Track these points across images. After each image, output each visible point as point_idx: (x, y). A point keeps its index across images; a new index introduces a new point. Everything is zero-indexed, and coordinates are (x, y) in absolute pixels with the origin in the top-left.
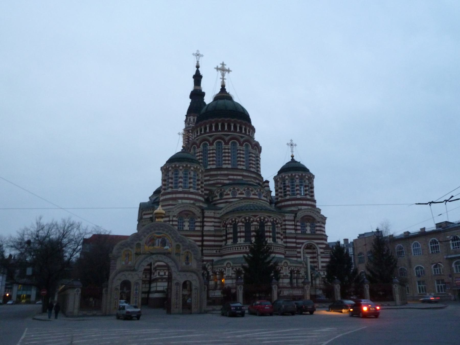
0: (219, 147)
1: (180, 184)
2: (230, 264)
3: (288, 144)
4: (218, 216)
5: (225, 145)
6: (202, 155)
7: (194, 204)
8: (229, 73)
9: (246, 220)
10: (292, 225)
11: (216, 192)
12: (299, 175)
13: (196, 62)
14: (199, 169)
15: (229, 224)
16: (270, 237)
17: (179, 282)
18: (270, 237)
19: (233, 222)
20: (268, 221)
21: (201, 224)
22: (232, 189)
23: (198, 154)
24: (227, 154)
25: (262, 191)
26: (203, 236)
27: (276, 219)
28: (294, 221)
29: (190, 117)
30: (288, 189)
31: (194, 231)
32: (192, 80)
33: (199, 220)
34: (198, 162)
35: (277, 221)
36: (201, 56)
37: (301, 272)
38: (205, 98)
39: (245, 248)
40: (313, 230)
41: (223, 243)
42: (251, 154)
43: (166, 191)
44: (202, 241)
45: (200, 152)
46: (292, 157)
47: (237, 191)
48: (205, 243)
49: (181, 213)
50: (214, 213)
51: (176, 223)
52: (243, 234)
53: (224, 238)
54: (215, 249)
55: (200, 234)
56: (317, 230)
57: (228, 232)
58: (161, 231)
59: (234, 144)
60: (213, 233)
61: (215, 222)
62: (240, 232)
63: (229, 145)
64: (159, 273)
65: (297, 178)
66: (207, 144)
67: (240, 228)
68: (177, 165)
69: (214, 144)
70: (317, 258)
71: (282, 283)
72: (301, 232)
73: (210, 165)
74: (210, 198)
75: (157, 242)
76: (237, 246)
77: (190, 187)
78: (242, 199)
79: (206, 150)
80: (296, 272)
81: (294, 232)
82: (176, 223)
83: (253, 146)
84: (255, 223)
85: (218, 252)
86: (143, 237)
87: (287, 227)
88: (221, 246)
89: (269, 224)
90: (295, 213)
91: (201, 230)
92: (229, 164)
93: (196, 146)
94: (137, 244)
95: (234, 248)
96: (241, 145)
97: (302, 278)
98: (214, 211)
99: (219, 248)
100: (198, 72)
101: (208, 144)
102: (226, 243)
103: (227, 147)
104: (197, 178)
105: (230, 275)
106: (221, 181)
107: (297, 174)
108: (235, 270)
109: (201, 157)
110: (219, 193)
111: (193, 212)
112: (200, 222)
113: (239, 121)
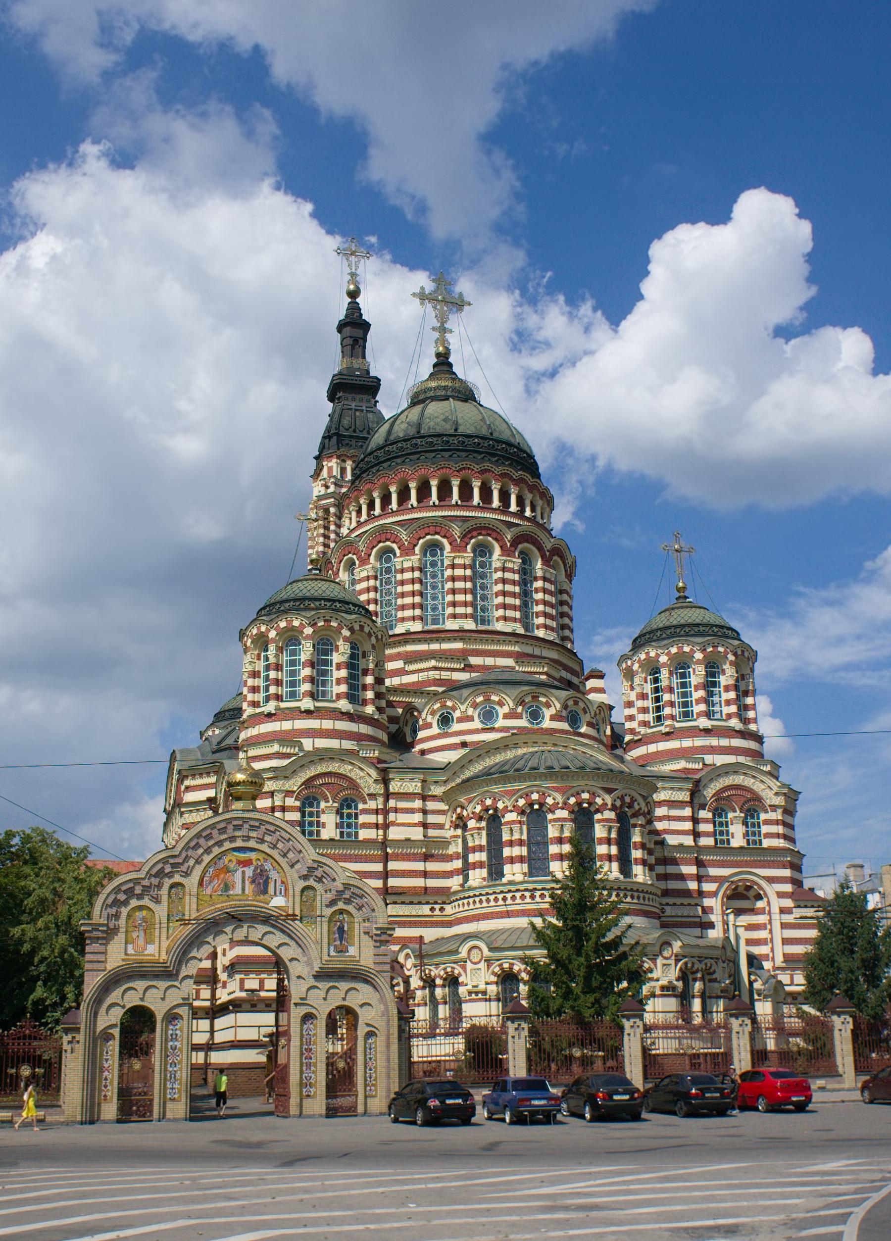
0: (432, 559)
2: (480, 949)
5: (453, 555)
6: (376, 589)
11: (426, 711)
13: (349, 277)
14: (370, 635)
15: (472, 818)
16: (609, 858)
17: (314, 1011)
23: (364, 585)
26: (386, 858)
27: (633, 800)
28: (691, 803)
29: (330, 464)
33: (372, 805)
34: (367, 611)
35: (636, 807)
37: (714, 976)
39: (528, 897)
40: (754, 834)
41: (454, 883)
43: (258, 710)
45: (368, 578)
47: (497, 707)
48: (392, 882)
50: (424, 781)
54: (428, 903)
57: (470, 844)
58: (252, 844)
61: (425, 812)
62: (511, 844)
63: (465, 551)
64: (242, 981)
66: (392, 551)
67: (511, 830)
69: (417, 549)
70: (769, 927)
71: (655, 1012)
72: (716, 840)
73: (403, 620)
74: (408, 730)
75: (238, 876)
76: (502, 892)
78: (513, 734)
79: (388, 571)
80: (699, 975)
81: (693, 844)
83: (548, 554)
85: (437, 912)
86: (191, 862)
88: (444, 892)
89: (612, 815)
91: (380, 837)
92: (466, 616)
93: (354, 557)
94: (172, 886)
95: (492, 897)
97: (719, 994)
98: (422, 777)
101: (398, 552)
102: (466, 879)
103: (457, 561)
105: (482, 987)
106: (443, 673)
108: (497, 970)
109: (372, 595)
110: (437, 717)
112: (377, 812)
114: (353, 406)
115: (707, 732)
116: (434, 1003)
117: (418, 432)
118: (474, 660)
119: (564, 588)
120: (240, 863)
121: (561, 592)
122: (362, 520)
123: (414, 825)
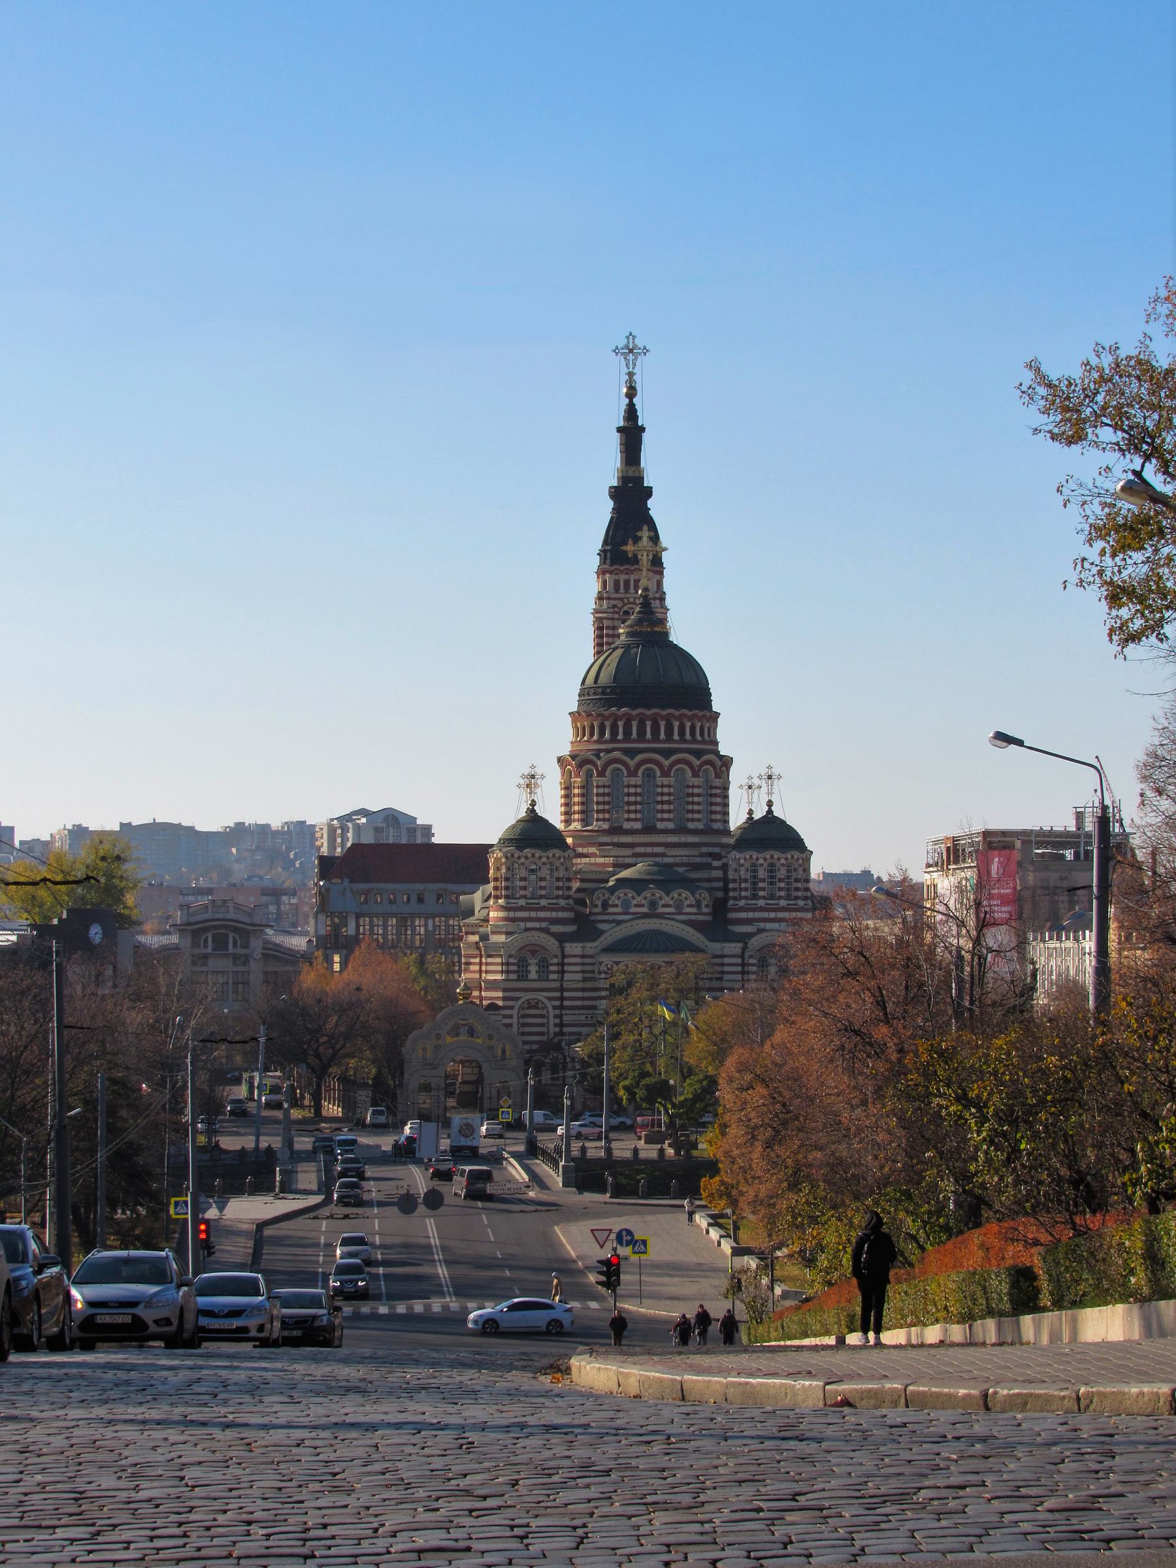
4: (591, 952)
10: (737, 965)
12: (765, 859)
13: (627, 377)
14: (559, 858)
19: (608, 969)
22: (622, 895)
24: (632, 799)
29: (607, 576)
30: (743, 885)
31: (548, 980)
32: (614, 442)
33: (555, 961)
36: (640, 354)
42: (690, 791)
44: (562, 999)
46: (770, 804)
48: (566, 1003)
49: (522, 948)
51: (514, 968)
55: (556, 985)
59: (649, 774)
60: (580, 985)
61: (583, 964)
63: (636, 776)
65: (761, 865)
77: (541, 897)
82: (514, 968)
87: (727, 969)
88: (594, 1008)
90: (744, 938)
92: (636, 820)
96: (665, 774)
98: (581, 945)
99: (590, 1012)
100: (631, 413)
104: (556, 874)
106: (619, 859)
107: (763, 858)
110: (601, 900)
111: (544, 948)
112: (558, 964)
113: (664, 713)
115: (762, 909)
120: (464, 1025)
121: (711, 788)
123: (577, 972)
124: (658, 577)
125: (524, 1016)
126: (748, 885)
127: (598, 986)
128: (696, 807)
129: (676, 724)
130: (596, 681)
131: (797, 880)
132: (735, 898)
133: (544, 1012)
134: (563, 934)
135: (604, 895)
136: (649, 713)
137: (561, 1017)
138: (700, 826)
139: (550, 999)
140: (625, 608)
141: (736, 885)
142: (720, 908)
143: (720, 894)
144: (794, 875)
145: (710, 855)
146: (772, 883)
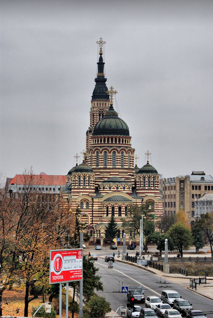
1: (81, 184)
3: (145, 154)
4: (101, 201)
7: (88, 195)
8: (115, 94)
9: (112, 206)
12: (148, 176)
16: (123, 214)
18: (123, 214)
19: (106, 206)
20: (123, 206)
21: (92, 205)
24: (110, 159)
25: (126, 186)
26: (93, 211)
28: (142, 202)
30: (141, 183)
32: (96, 67)
33: (91, 203)
38: (106, 83)
42: (125, 158)
43: (75, 187)
45: (94, 156)
46: (148, 162)
48: (94, 215)
52: (111, 212)
53: (103, 212)
55: (91, 210)
56: (155, 207)
59: (114, 153)
60: (98, 210)
61: (98, 204)
62: (109, 211)
63: (111, 153)
65: (147, 178)
68: (80, 174)
69: (103, 152)
73: (100, 165)
74: (99, 188)
79: (98, 155)
84: (116, 207)
88: (101, 216)
92: (111, 165)
96: (119, 153)
99: (101, 218)
100: (101, 59)
103: (109, 155)
112: (92, 204)
113: (118, 136)
114: (100, 87)
115: (147, 190)
116: (97, 233)
117: (104, 128)
118: (111, 173)
119: (131, 156)
121: (130, 157)
122: (94, 143)
124: (108, 102)
125: (82, 219)
126: (143, 183)
127: (103, 210)
128: (127, 162)
129: (121, 139)
130: (99, 128)
131: (156, 182)
132: (139, 187)
133: (88, 218)
134: (92, 196)
135: (103, 185)
136: (114, 136)
137: (92, 219)
138: (127, 167)
139: (89, 214)
140: (99, 111)
141: (139, 183)
142: (134, 189)
143: (134, 186)
144: (155, 180)
145: (130, 175)
146: (149, 183)
